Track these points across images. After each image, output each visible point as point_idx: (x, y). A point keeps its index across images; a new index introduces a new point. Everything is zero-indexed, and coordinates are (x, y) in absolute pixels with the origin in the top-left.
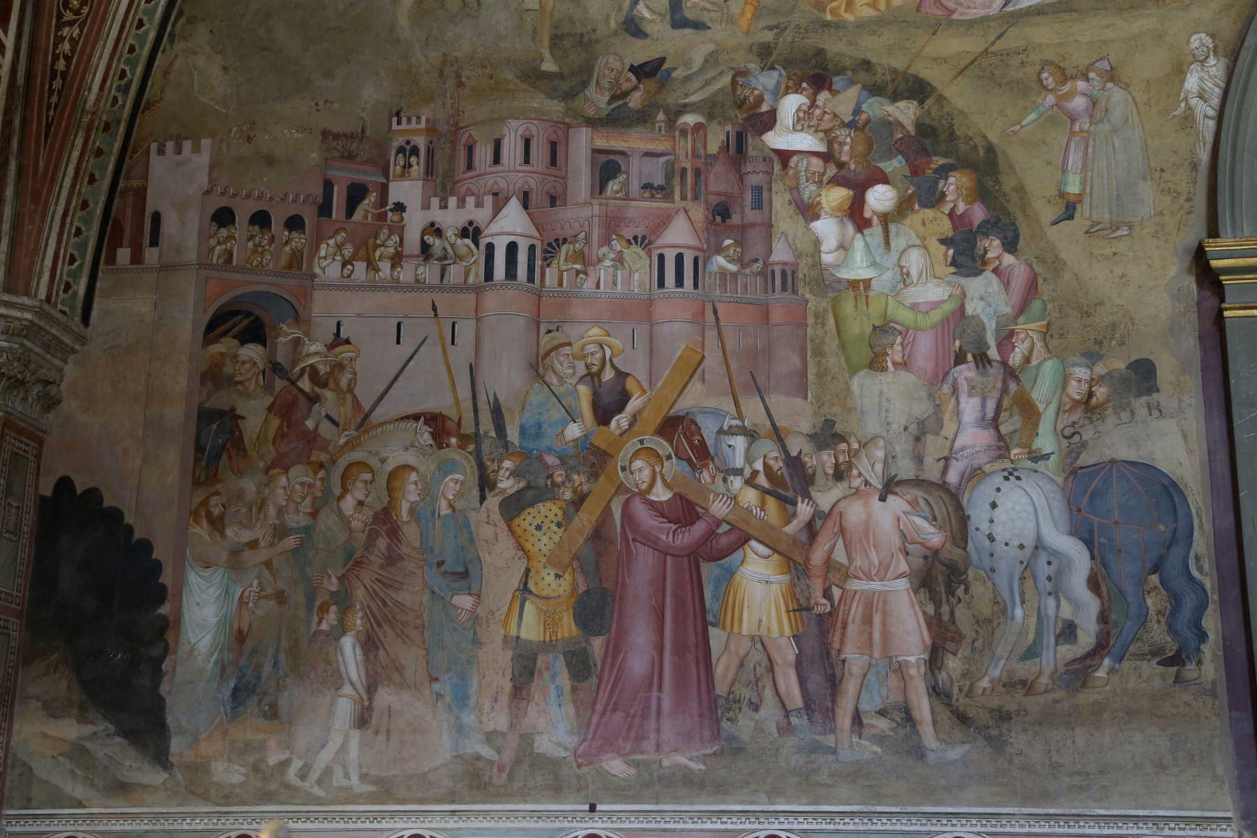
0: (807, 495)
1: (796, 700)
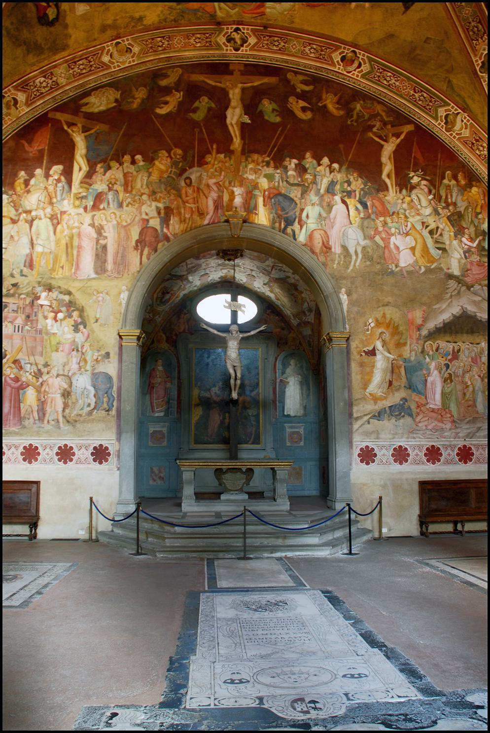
0: (41, 377)
1: (37, 418)
